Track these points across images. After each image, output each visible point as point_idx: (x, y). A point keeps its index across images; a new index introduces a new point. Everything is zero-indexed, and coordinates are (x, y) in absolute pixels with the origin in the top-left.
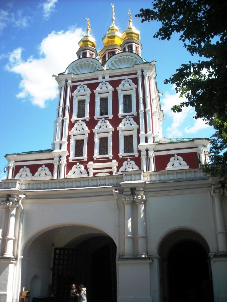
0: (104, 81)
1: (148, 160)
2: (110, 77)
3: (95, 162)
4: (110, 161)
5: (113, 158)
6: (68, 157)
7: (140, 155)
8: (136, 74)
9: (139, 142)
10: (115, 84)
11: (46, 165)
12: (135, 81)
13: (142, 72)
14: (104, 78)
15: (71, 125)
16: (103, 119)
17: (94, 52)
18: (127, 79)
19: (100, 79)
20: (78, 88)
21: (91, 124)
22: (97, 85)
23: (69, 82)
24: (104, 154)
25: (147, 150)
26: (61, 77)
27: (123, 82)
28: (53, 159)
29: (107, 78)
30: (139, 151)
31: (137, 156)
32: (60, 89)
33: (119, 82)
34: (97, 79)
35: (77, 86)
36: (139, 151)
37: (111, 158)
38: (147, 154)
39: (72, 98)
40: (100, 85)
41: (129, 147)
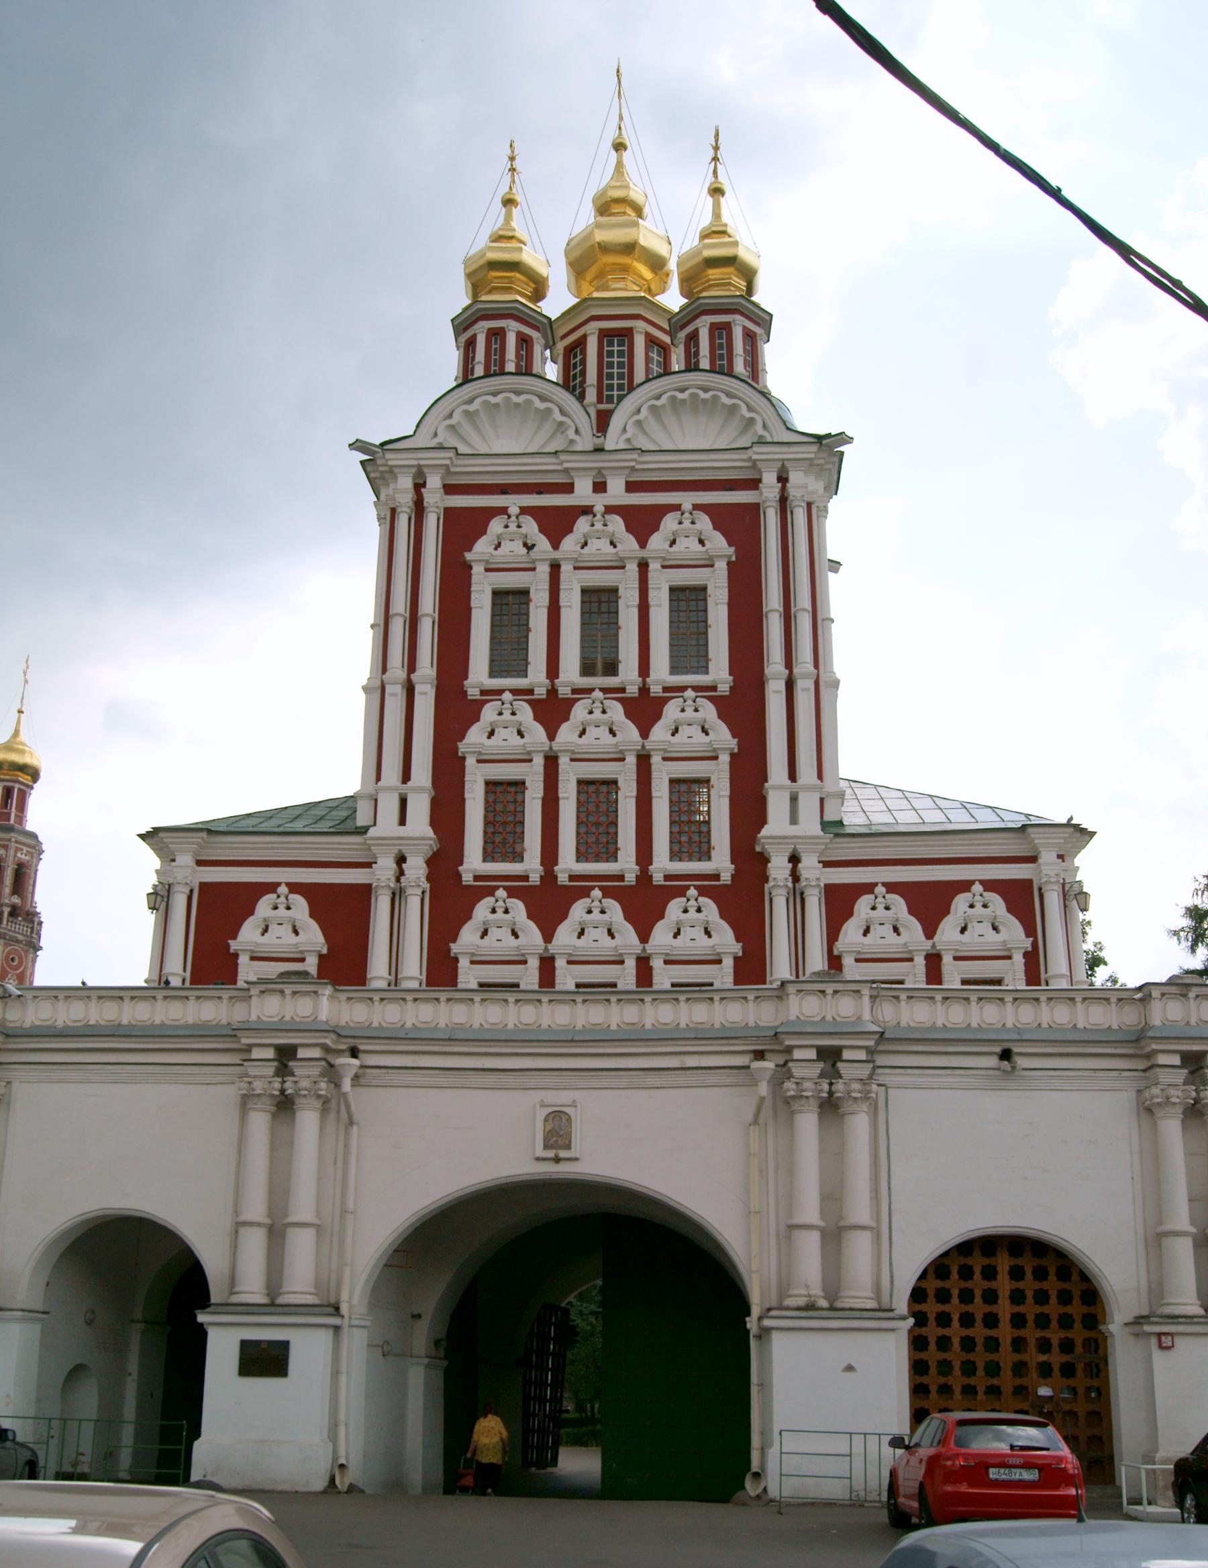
0: (599, 509)
1: (798, 897)
2: (631, 487)
8: (754, 484)
13: (783, 479)
14: (600, 487)
16: (598, 694)
17: (536, 328)
19: (583, 493)
24: (597, 858)
26: (394, 459)
28: (368, 865)
29: (616, 492)
32: (390, 518)
34: (568, 488)
38: (795, 877)
40: (582, 525)
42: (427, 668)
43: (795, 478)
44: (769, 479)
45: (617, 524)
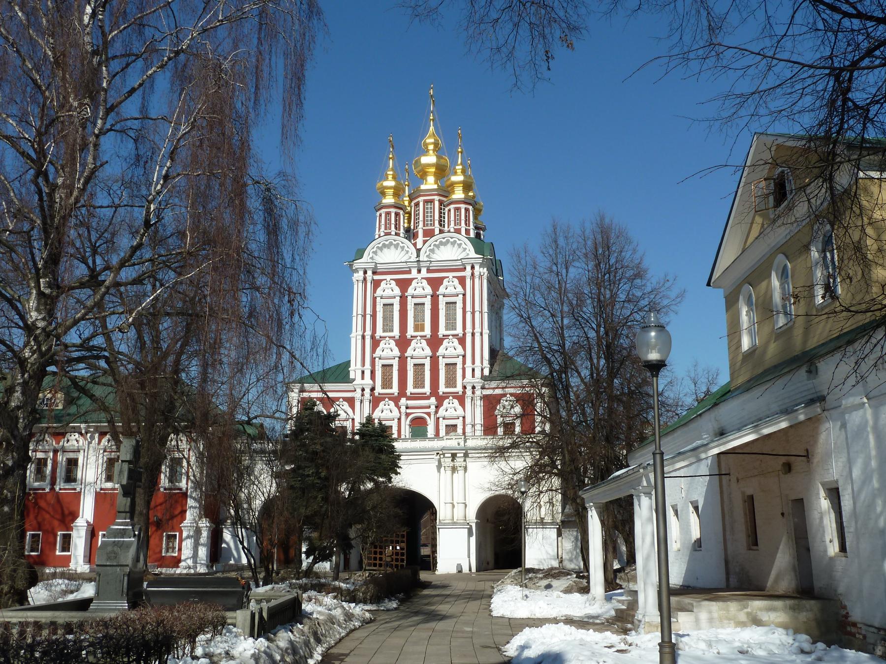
2: (429, 271)
3: (408, 398)
4: (428, 398)
5: (432, 394)
6: (373, 389)
7: (464, 393)
9: (464, 377)
10: (435, 283)
11: (345, 399)
12: (462, 281)
13: (473, 268)
14: (419, 271)
15: (375, 343)
18: (451, 277)
20: (383, 284)
21: (403, 343)
22: (409, 282)
23: (369, 273)
25: (474, 388)
27: (445, 282)
30: (465, 387)
31: (461, 393)
33: (440, 281)
34: (409, 272)
35: (382, 280)
36: (465, 387)
37: (428, 393)
39: (374, 299)
40: (414, 283)
41: (451, 382)
42: (368, 333)
43: (477, 267)
44: (469, 268)
45: (425, 282)
